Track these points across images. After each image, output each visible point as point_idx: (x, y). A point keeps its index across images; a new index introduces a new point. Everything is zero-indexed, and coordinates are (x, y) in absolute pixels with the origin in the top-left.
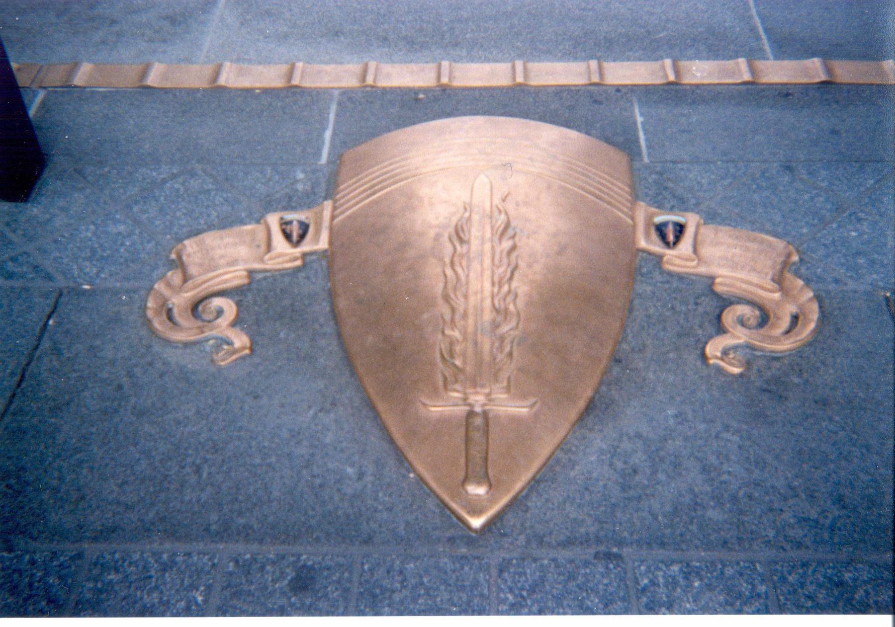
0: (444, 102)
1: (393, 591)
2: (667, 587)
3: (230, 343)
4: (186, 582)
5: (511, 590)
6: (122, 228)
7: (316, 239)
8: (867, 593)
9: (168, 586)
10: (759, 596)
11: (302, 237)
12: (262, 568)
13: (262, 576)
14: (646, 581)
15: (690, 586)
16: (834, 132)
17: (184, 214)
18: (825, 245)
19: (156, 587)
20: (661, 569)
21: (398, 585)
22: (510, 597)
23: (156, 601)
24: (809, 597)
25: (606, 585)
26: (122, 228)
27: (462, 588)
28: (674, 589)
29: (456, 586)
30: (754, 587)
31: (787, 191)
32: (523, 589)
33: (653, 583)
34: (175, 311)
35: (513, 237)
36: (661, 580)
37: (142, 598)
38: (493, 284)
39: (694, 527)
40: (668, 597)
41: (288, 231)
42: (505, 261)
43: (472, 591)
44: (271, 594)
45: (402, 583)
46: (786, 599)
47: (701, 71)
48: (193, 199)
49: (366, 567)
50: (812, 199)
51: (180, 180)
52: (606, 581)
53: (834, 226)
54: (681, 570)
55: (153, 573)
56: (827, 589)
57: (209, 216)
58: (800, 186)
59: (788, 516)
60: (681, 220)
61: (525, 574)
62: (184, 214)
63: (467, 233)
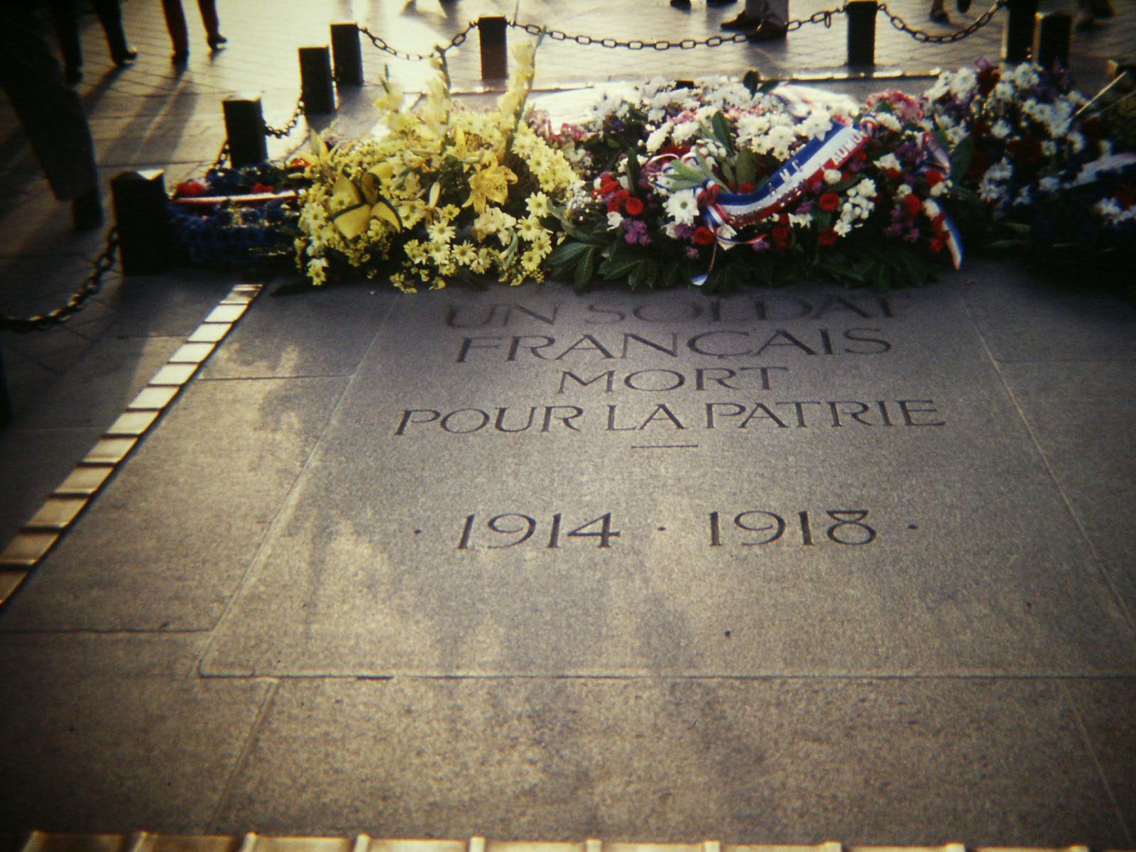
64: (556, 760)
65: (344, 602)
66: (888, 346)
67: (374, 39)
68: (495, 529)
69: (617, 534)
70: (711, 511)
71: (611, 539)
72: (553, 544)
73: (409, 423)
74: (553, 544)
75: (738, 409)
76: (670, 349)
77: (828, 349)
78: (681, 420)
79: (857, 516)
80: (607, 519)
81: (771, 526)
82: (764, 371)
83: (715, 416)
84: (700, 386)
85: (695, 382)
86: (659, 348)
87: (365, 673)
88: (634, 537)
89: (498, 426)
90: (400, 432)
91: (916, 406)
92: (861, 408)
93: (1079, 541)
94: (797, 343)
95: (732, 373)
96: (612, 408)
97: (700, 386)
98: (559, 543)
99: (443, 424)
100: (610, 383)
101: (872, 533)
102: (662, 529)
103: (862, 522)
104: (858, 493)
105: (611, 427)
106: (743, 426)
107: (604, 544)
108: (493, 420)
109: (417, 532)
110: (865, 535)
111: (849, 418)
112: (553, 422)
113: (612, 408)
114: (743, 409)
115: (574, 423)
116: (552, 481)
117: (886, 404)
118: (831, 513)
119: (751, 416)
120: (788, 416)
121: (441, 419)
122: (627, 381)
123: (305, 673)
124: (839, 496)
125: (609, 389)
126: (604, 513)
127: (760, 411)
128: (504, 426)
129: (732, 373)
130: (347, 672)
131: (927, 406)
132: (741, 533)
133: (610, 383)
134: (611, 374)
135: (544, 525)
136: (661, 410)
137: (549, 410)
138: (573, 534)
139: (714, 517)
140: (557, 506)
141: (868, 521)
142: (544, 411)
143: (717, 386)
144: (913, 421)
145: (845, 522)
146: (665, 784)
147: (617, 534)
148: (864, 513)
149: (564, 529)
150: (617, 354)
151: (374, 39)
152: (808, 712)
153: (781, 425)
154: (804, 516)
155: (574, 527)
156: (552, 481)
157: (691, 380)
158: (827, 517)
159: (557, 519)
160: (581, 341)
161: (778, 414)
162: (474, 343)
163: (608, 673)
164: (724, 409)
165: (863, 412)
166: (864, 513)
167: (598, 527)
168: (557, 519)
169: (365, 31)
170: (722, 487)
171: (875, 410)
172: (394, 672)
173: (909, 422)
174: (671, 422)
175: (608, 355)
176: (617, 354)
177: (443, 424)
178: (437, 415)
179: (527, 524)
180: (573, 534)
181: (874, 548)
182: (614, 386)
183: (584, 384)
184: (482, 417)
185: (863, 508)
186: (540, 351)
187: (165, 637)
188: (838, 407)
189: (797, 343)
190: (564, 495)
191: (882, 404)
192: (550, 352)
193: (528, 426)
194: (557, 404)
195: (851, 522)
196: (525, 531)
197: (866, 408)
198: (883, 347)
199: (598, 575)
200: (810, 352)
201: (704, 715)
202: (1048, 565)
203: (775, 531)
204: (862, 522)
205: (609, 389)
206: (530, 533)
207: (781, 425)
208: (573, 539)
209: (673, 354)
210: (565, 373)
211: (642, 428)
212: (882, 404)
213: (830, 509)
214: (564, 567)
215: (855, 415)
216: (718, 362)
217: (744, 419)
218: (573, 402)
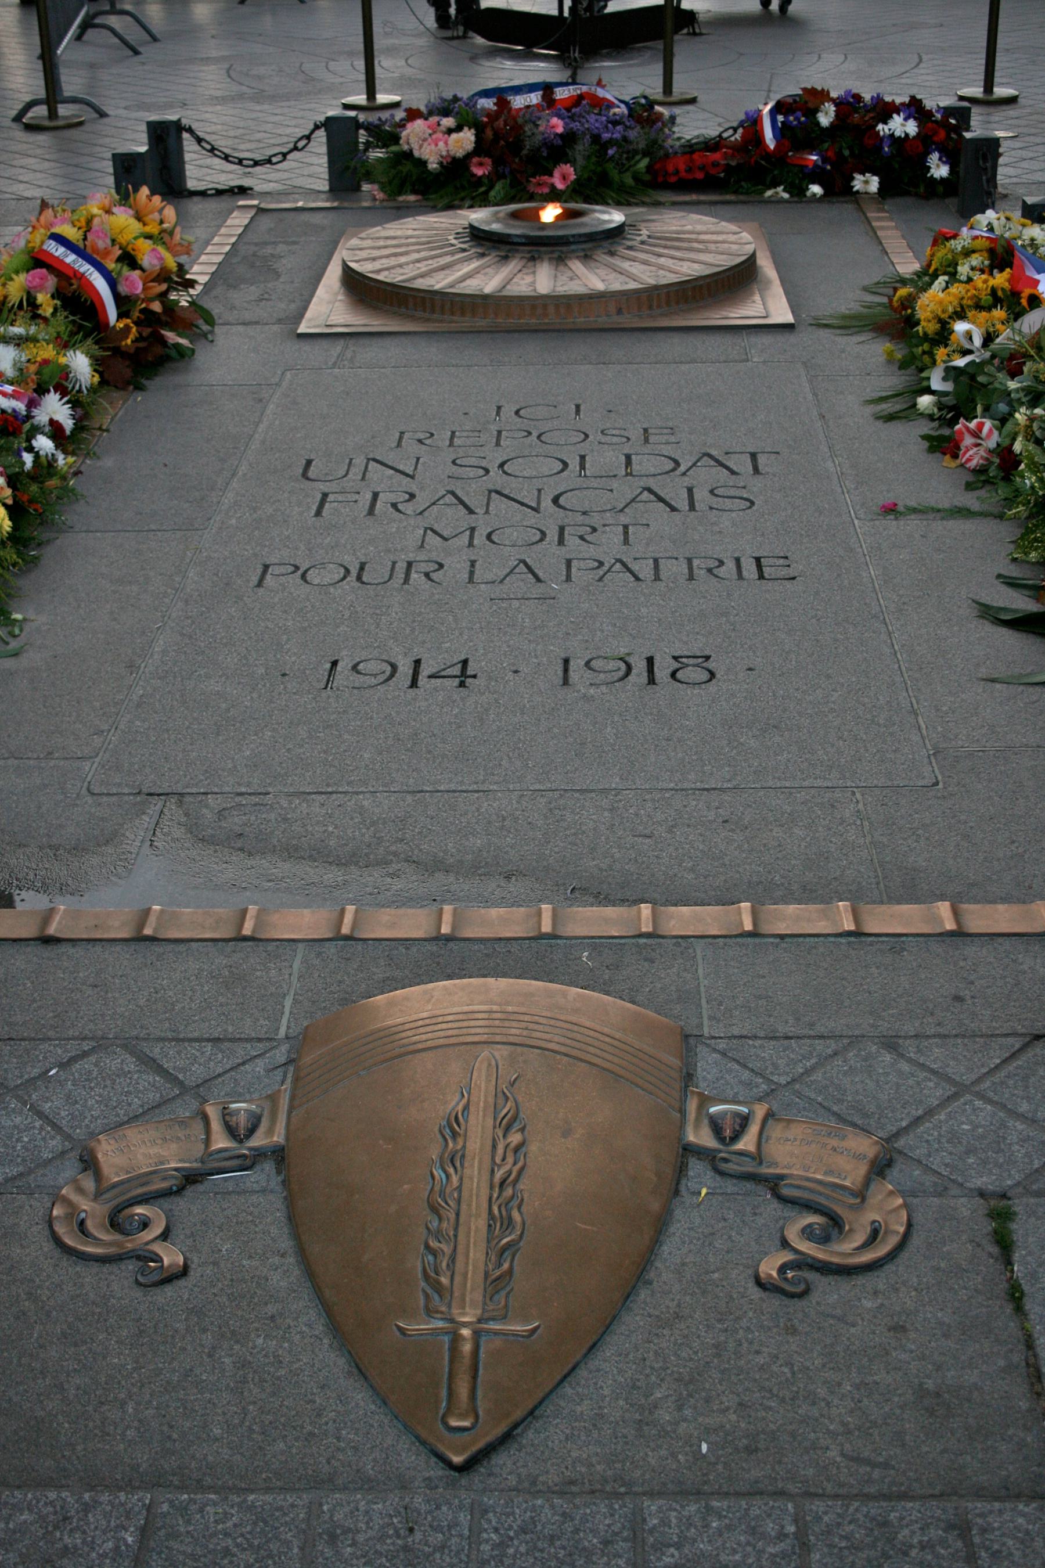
0: (447, 956)
1: (358, 1532)
2: (679, 1527)
3: (158, 1259)
4: (113, 1524)
5: (496, 1530)
6: (18, 1120)
7: (270, 1132)
8: (913, 1532)
9: (92, 1527)
10: (786, 1536)
11: (251, 1131)
12: (201, 1510)
13: (203, 1517)
14: (655, 1521)
15: (707, 1526)
16: (958, 999)
17: (97, 1102)
18: (927, 1141)
19: (78, 1528)
20: (675, 1510)
21: (364, 1527)
22: (493, 1536)
23: (79, 1541)
24: (846, 1538)
25: (609, 1526)
26: (18, 1120)
27: (438, 1529)
28: (688, 1529)
29: (431, 1526)
30: (783, 1527)
31: (887, 1074)
32: (510, 1528)
33: (665, 1522)
34: (90, 1224)
35: (522, 1130)
36: (674, 1521)
37: (61, 1539)
38: (492, 1187)
39: (720, 1467)
40: (680, 1537)
41: (233, 1124)
42: (510, 1160)
43: (449, 1530)
44: (215, 1534)
45: (367, 1523)
46: (818, 1539)
47: (790, 917)
48: (108, 1082)
49: (325, 1508)
50: (918, 1083)
51: (93, 1059)
52: (607, 1522)
53: (942, 1117)
54: (698, 1510)
55: (73, 1513)
56: (866, 1528)
57: (130, 1105)
58: (905, 1067)
59: (833, 1453)
60: (745, 1110)
61: (513, 1513)
62: (97, 1102)
63: (463, 1128)
64: (416, 852)
65: (218, 734)
66: (752, 503)
67: (199, 141)
68: (358, 672)
69: (474, 676)
70: (563, 656)
71: (469, 680)
72: (414, 684)
73: (268, 577)
74: (414, 684)
75: (596, 564)
76: (534, 505)
77: (692, 507)
78: (541, 574)
79: (700, 660)
80: (465, 663)
81: (619, 669)
82: (626, 527)
83: (574, 570)
84: (561, 541)
85: (556, 538)
86: (522, 504)
87: (243, 790)
88: (490, 678)
89: (359, 578)
90: (260, 584)
91: (771, 561)
92: (717, 563)
93: (898, 679)
94: (661, 499)
95: (594, 530)
96: (473, 563)
97: (561, 541)
98: (420, 683)
99: (303, 576)
100: (472, 537)
101: (712, 675)
102: (516, 672)
103: (704, 665)
104: (704, 640)
105: (471, 580)
106: (601, 579)
107: (462, 684)
108: (354, 573)
109: (284, 675)
110: (706, 676)
111: (702, 572)
112: (414, 576)
113: (473, 563)
114: (601, 564)
115: (433, 576)
116: (413, 630)
117: (742, 560)
118: (675, 658)
119: (608, 571)
120: (645, 570)
121: (299, 573)
122: (489, 537)
123: (188, 790)
124: (686, 643)
125: (471, 544)
126: (463, 657)
127: (618, 566)
128: (364, 579)
129: (594, 530)
130: (227, 789)
131: (781, 561)
132: (588, 674)
133: (472, 537)
134: (473, 530)
135: (405, 668)
136: (521, 565)
137: (410, 564)
138: (429, 677)
139: (566, 661)
140: (418, 652)
141: (711, 665)
142: (405, 565)
143: (578, 541)
144: (766, 575)
145: (688, 665)
146: (509, 868)
147: (474, 676)
148: (707, 658)
149: (425, 671)
150: (481, 511)
151: (199, 141)
152: (637, 815)
153: (637, 579)
154: (650, 661)
155: (434, 671)
156: (413, 630)
157: (553, 535)
158: (672, 661)
159: (418, 663)
160: (444, 496)
161: (635, 567)
162: (331, 498)
163: (464, 788)
164: (582, 564)
165: (718, 567)
166: (707, 658)
167: (456, 670)
168: (418, 663)
169: (190, 130)
170: (575, 635)
171: (731, 565)
172: (270, 789)
173: (761, 576)
174: (530, 576)
175: (471, 512)
176: (481, 511)
177: (303, 576)
178: (297, 568)
179: (388, 669)
180: (429, 677)
181: (712, 687)
182: (476, 542)
183: (446, 539)
184: (342, 571)
185: (707, 653)
186: (400, 506)
187: (52, 763)
188: (696, 563)
189: (661, 499)
190: (424, 642)
191: (738, 560)
192: (409, 508)
193: (390, 578)
194: (418, 559)
195: (694, 666)
196: (388, 673)
197: (721, 563)
198: (748, 504)
199: (456, 711)
200: (673, 509)
201: (546, 818)
202: (866, 700)
203: (621, 673)
204: (704, 665)
205: (471, 544)
206: (392, 676)
207: (637, 579)
208: (433, 681)
209: (536, 510)
210: (426, 529)
211: (501, 582)
212: (738, 560)
213: (676, 655)
214: (424, 704)
215: (710, 571)
216: (580, 518)
217: (601, 573)
218: (434, 556)
